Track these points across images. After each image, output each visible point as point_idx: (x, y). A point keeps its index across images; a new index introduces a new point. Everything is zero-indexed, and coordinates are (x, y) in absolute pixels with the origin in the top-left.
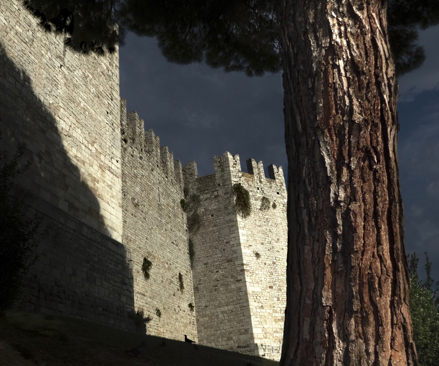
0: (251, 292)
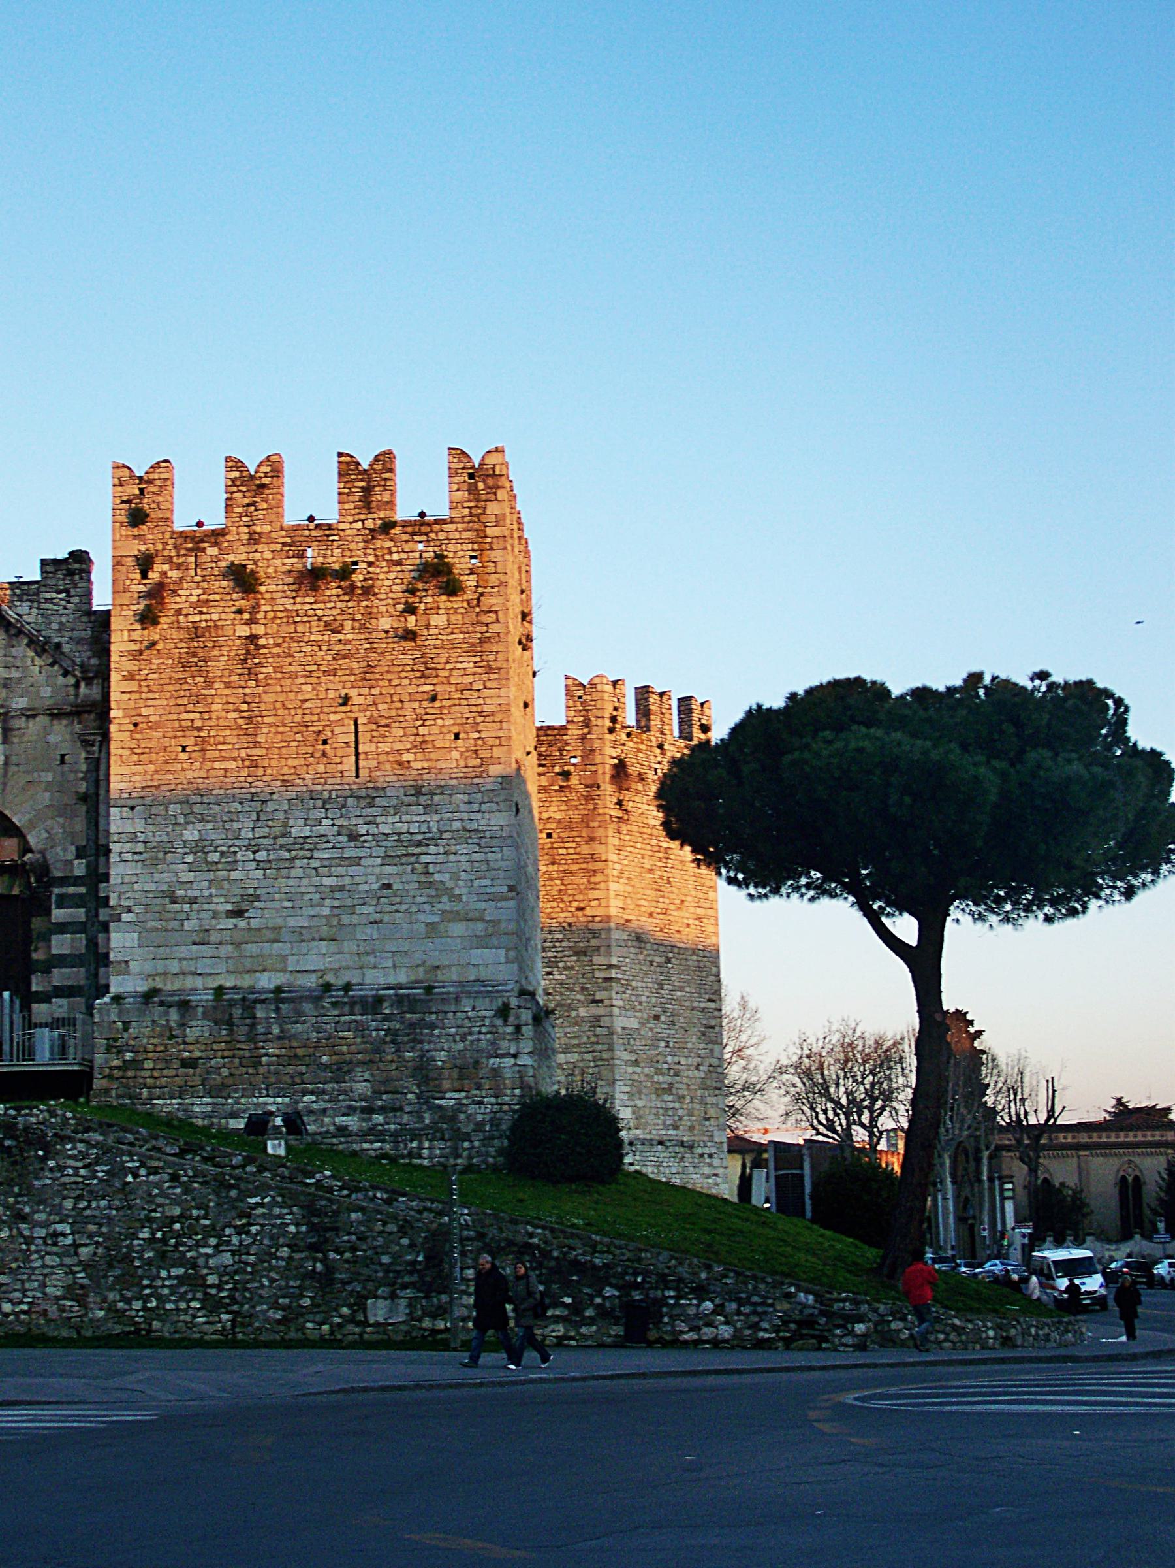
0: (619, 1030)
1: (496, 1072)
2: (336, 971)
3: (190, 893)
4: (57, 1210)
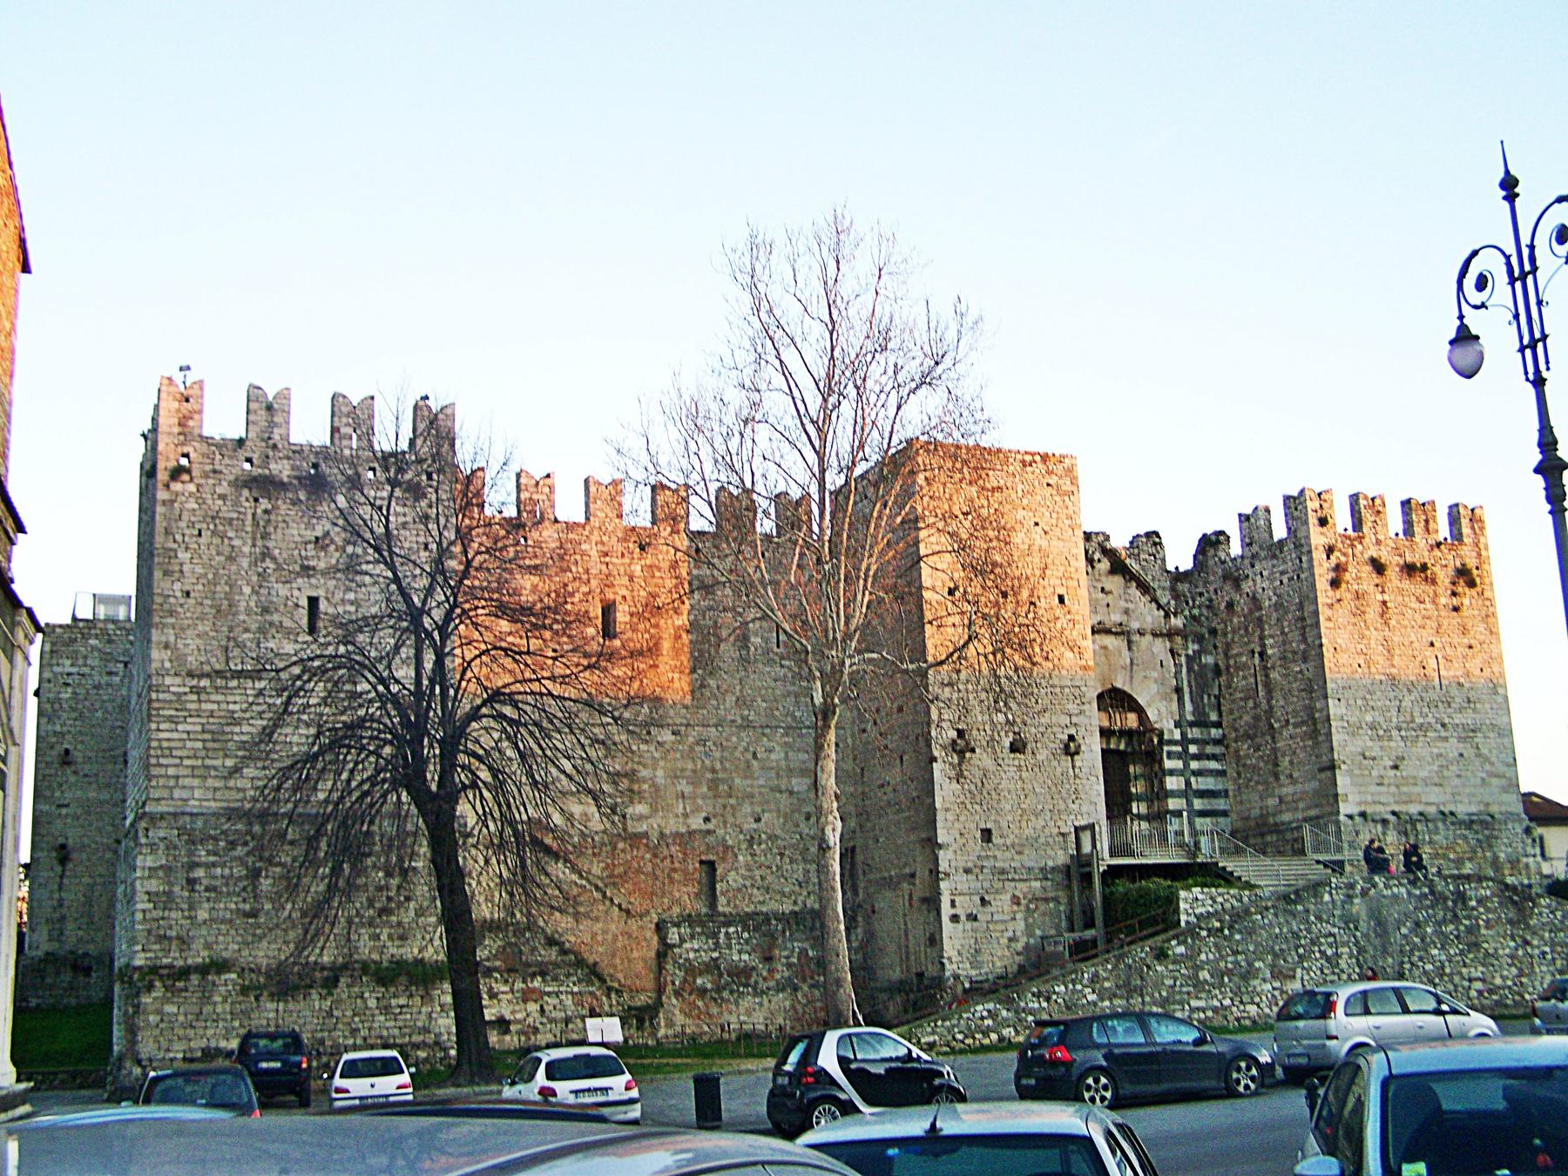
1: (1527, 866)
2: (1444, 804)
3: (1373, 754)
4: (1542, 938)
